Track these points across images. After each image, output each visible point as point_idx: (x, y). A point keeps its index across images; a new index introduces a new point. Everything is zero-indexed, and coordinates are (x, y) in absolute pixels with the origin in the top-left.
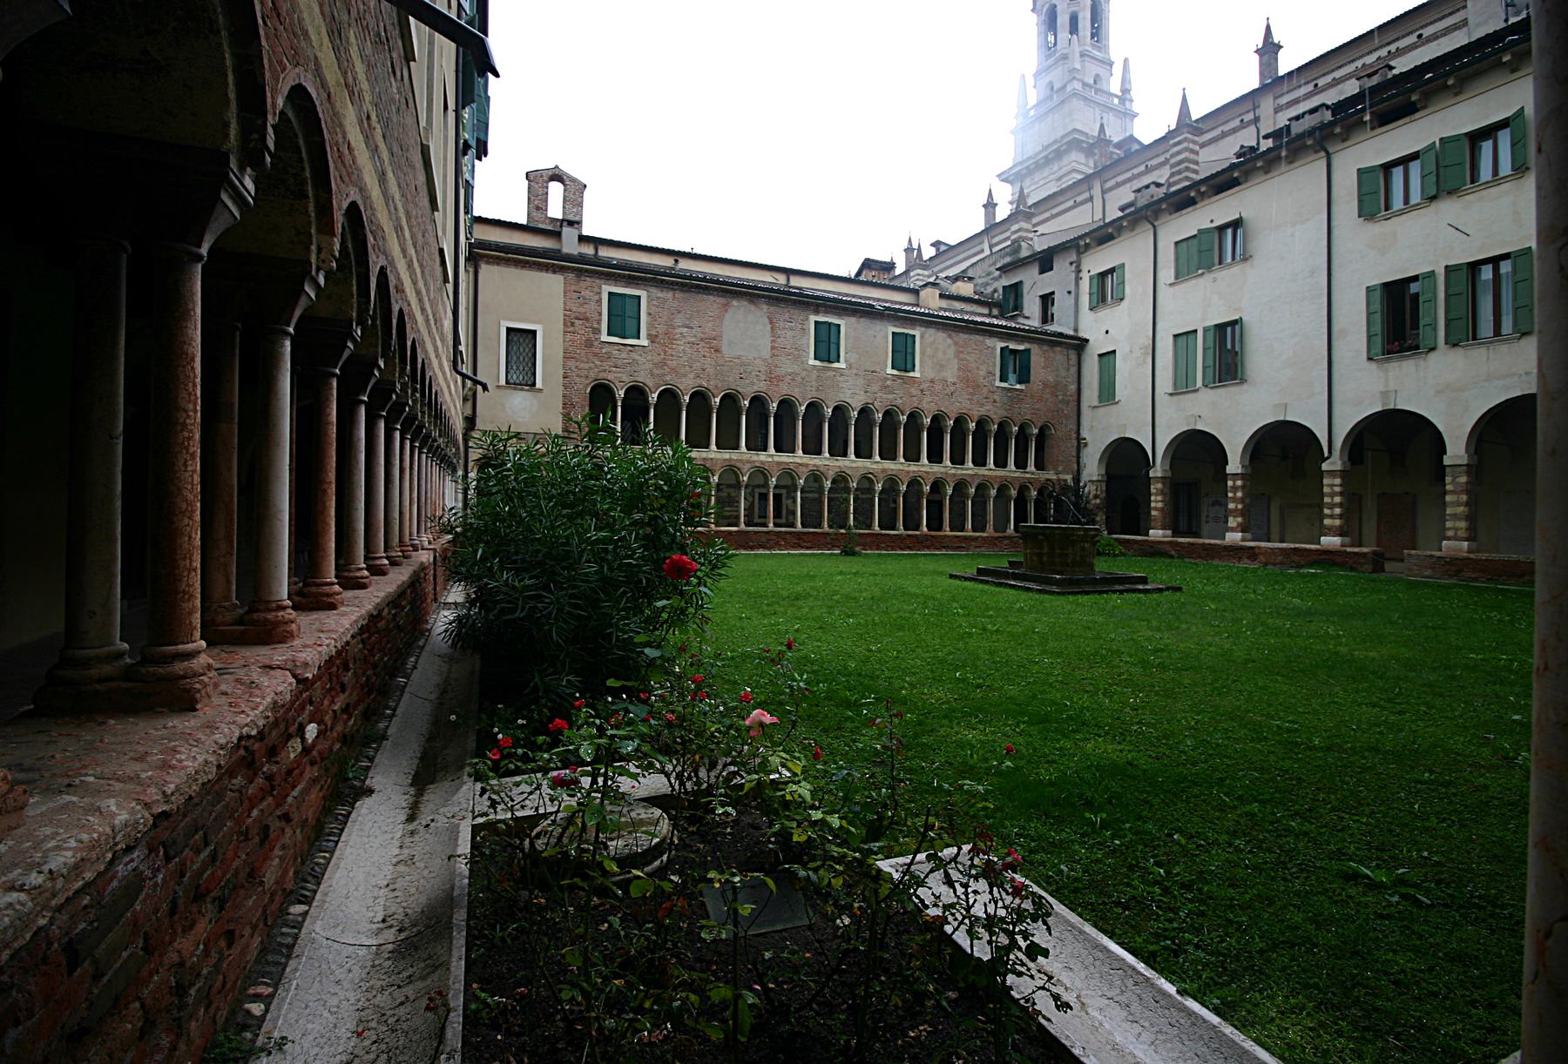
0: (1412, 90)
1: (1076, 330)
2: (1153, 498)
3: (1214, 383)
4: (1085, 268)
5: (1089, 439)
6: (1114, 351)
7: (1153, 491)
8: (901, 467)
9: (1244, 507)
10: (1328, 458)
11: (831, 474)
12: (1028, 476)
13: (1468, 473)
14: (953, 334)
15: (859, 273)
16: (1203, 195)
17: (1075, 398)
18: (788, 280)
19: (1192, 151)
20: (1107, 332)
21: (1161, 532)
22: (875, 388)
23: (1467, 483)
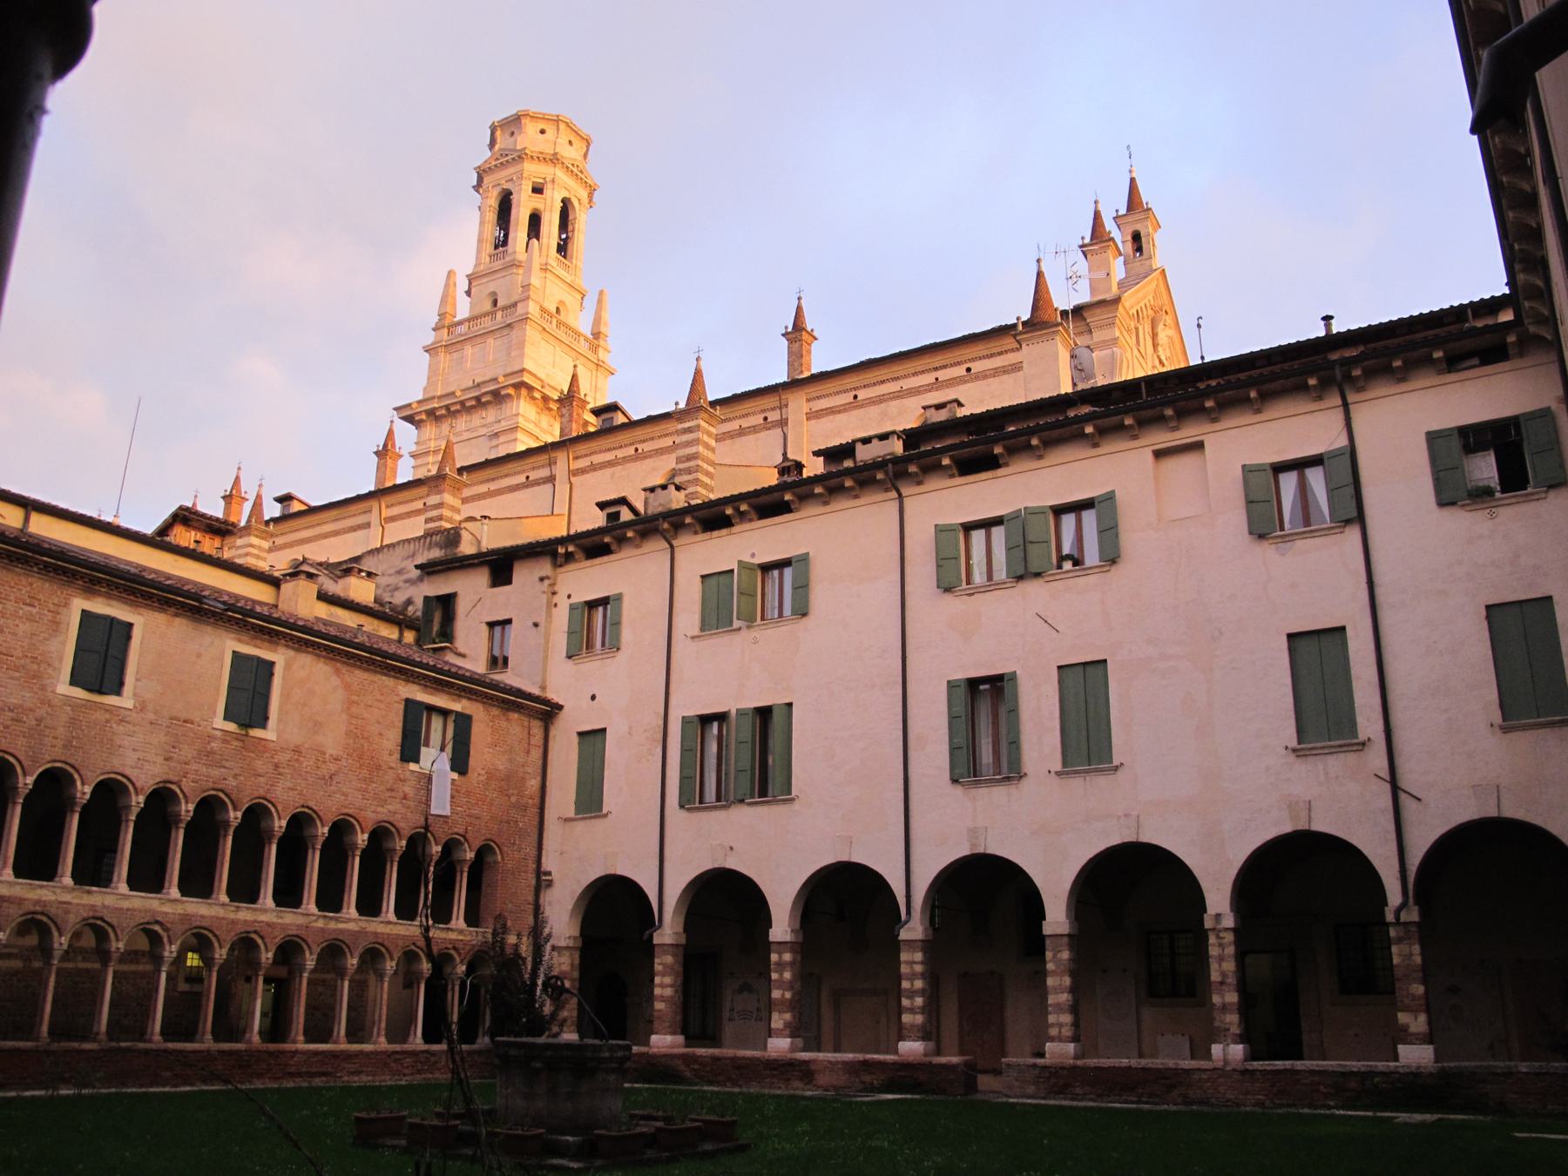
0: (995, 441)
1: (543, 688)
2: (657, 980)
3: (752, 796)
4: (562, 591)
5: (555, 876)
6: (604, 730)
7: (658, 968)
8: (220, 912)
9: (793, 996)
10: (907, 922)
11: (72, 921)
12: (453, 936)
13: (1071, 947)
14: (344, 669)
15: (164, 530)
16: (742, 516)
17: (537, 801)
18: (27, 520)
19: (707, 446)
20: (593, 698)
21: (669, 1038)
22: (187, 752)
23: (1070, 960)
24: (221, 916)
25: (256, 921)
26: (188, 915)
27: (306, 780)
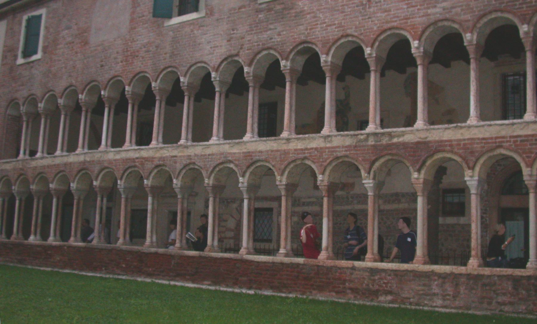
22: (242, 29)
24: (275, 149)
25: (306, 149)
26: (249, 152)
27: (342, 12)
